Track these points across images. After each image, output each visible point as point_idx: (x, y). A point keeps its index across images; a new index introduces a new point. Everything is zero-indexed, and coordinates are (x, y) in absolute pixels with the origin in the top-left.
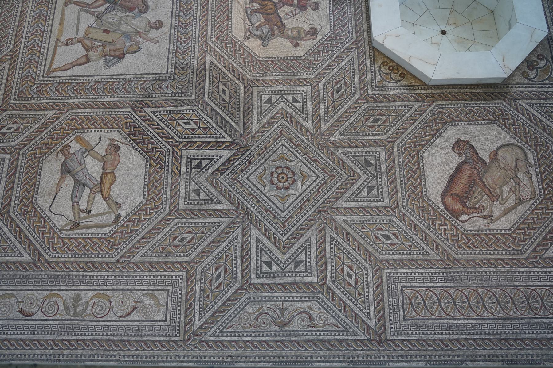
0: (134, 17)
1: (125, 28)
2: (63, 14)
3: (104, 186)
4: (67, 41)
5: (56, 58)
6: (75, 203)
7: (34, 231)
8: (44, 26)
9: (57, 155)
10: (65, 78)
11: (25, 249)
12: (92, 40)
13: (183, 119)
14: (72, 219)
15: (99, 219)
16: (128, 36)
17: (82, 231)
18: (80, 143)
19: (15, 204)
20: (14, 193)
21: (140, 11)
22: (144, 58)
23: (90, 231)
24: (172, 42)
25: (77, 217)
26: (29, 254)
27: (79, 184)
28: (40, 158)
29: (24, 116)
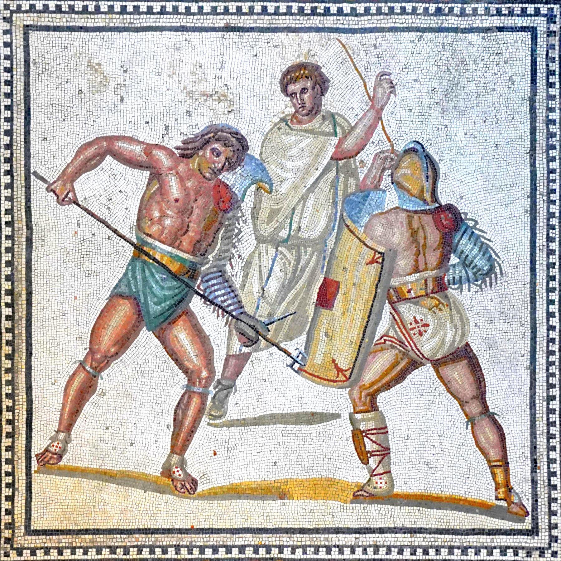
0: (264, 184)
1: (315, 220)
2: (235, 492)
10: (542, 441)
12: (364, 349)
16: (353, 204)
21: (230, 165)
24: (388, 22)
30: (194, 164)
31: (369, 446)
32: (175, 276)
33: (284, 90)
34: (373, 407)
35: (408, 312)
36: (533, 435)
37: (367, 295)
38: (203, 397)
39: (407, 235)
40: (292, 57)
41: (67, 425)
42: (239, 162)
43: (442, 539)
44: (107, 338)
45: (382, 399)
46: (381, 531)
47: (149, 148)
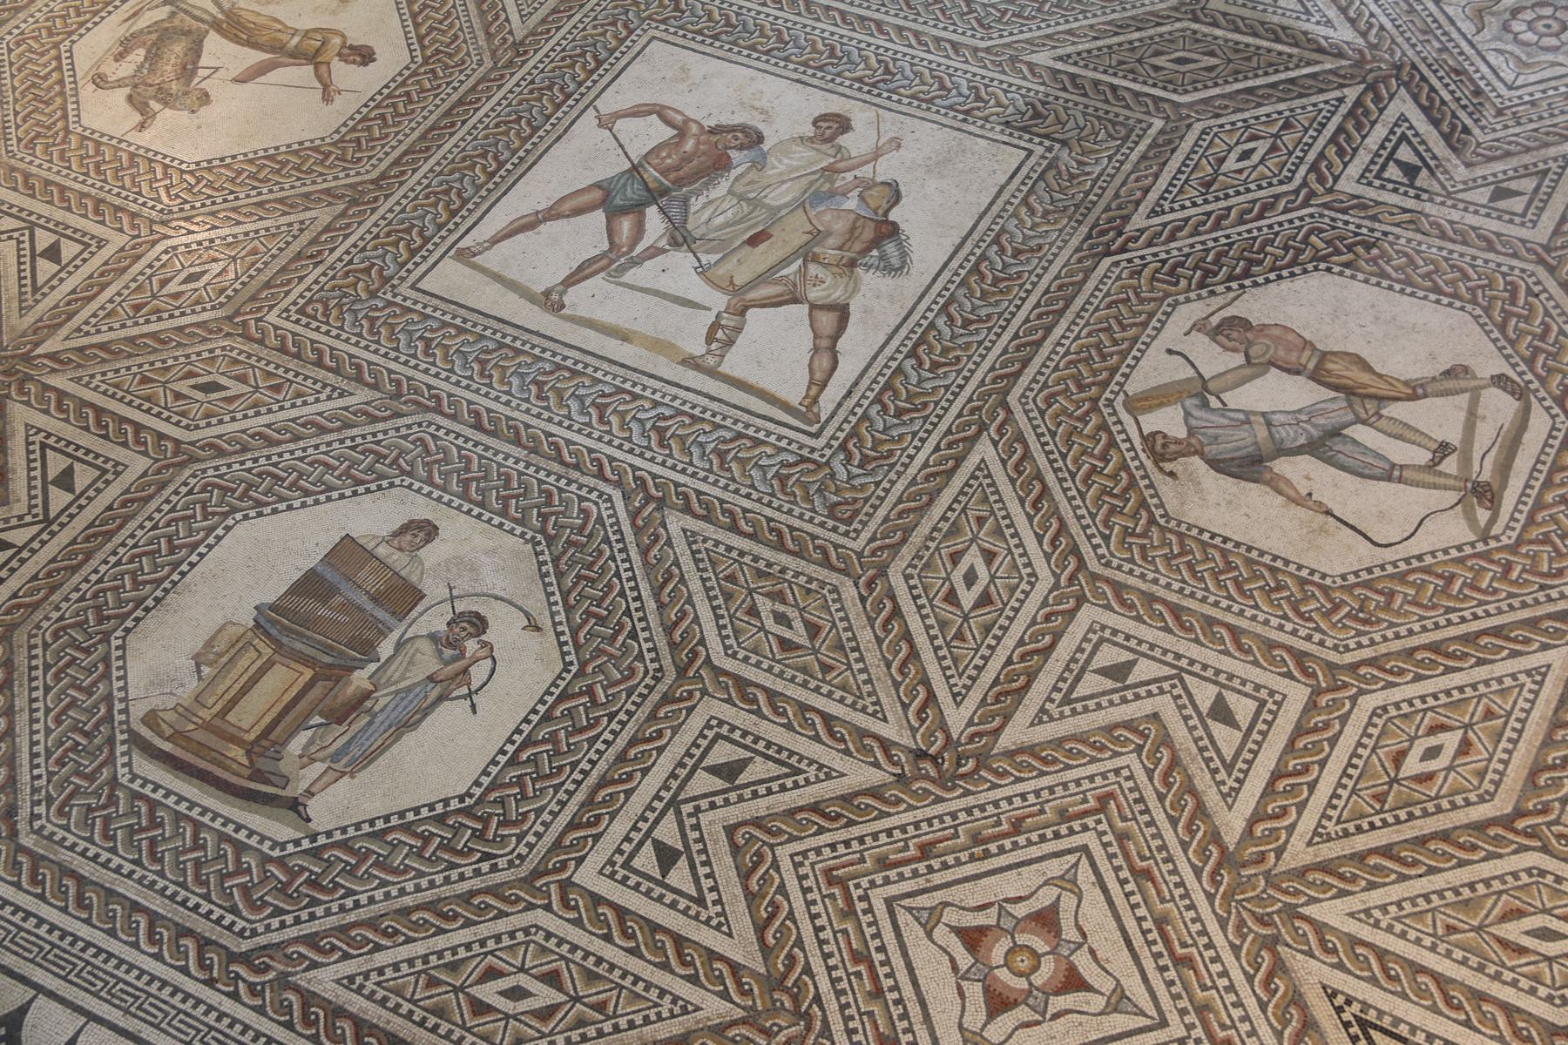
0: (759, 164)
1: (780, 196)
2: (590, 324)
3: (1365, 386)
4: (710, 338)
5: (761, 385)
6: (1391, 473)
7: (1449, 610)
8: (597, 381)
9: (1172, 474)
10: (865, 382)
11: (1515, 654)
13: (1222, 161)
14: (1452, 497)
15: (1485, 434)
17: (1516, 484)
18: (1161, 405)
19: (1309, 638)
20: (1259, 629)
21: (741, 148)
22: (932, 184)
23: (1523, 463)
25: (1451, 482)
26: (1545, 647)
27: (1323, 444)
28: (1152, 521)
29: (945, 526)
30: (714, 139)
31: (720, 334)
32: (648, 189)
33: (815, 123)
34: (742, 313)
35: (813, 269)
36: (861, 376)
37: (789, 250)
38: (612, 262)
39: (848, 226)
40: (834, 109)
41: (495, 241)
42: (750, 147)
43: (733, 412)
44: (567, 206)
45: (750, 313)
46: (687, 389)
47: (687, 120)
